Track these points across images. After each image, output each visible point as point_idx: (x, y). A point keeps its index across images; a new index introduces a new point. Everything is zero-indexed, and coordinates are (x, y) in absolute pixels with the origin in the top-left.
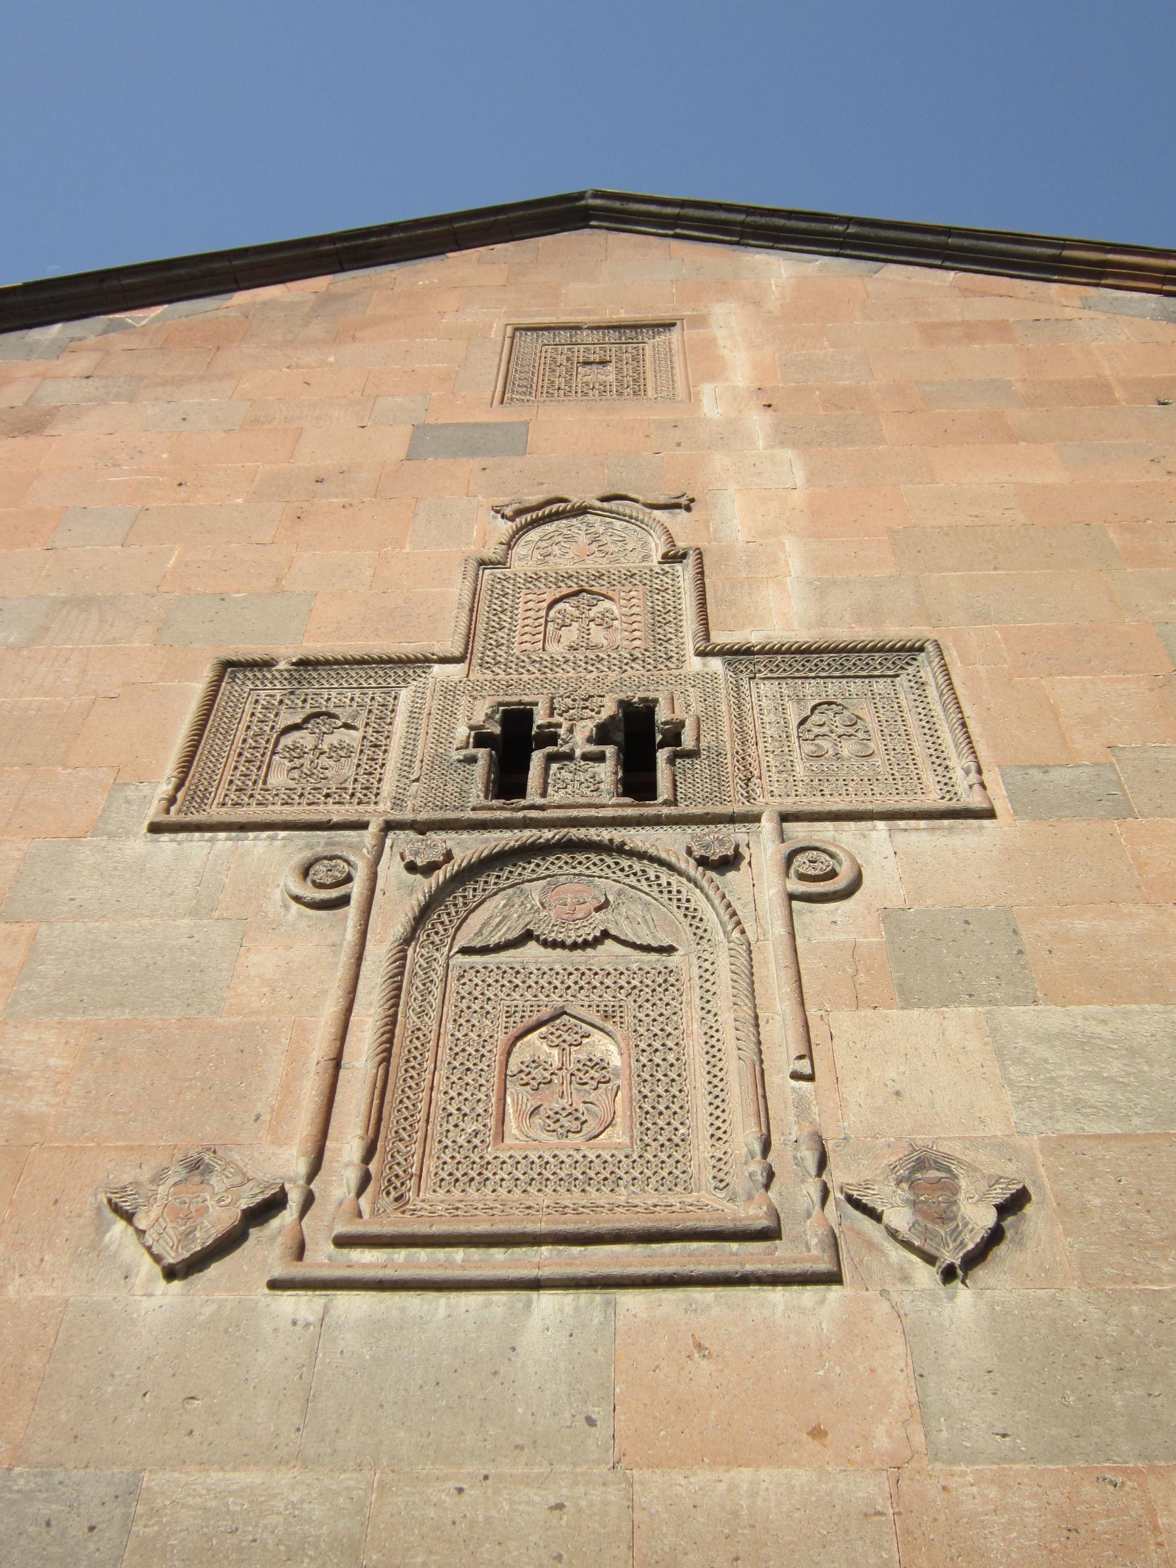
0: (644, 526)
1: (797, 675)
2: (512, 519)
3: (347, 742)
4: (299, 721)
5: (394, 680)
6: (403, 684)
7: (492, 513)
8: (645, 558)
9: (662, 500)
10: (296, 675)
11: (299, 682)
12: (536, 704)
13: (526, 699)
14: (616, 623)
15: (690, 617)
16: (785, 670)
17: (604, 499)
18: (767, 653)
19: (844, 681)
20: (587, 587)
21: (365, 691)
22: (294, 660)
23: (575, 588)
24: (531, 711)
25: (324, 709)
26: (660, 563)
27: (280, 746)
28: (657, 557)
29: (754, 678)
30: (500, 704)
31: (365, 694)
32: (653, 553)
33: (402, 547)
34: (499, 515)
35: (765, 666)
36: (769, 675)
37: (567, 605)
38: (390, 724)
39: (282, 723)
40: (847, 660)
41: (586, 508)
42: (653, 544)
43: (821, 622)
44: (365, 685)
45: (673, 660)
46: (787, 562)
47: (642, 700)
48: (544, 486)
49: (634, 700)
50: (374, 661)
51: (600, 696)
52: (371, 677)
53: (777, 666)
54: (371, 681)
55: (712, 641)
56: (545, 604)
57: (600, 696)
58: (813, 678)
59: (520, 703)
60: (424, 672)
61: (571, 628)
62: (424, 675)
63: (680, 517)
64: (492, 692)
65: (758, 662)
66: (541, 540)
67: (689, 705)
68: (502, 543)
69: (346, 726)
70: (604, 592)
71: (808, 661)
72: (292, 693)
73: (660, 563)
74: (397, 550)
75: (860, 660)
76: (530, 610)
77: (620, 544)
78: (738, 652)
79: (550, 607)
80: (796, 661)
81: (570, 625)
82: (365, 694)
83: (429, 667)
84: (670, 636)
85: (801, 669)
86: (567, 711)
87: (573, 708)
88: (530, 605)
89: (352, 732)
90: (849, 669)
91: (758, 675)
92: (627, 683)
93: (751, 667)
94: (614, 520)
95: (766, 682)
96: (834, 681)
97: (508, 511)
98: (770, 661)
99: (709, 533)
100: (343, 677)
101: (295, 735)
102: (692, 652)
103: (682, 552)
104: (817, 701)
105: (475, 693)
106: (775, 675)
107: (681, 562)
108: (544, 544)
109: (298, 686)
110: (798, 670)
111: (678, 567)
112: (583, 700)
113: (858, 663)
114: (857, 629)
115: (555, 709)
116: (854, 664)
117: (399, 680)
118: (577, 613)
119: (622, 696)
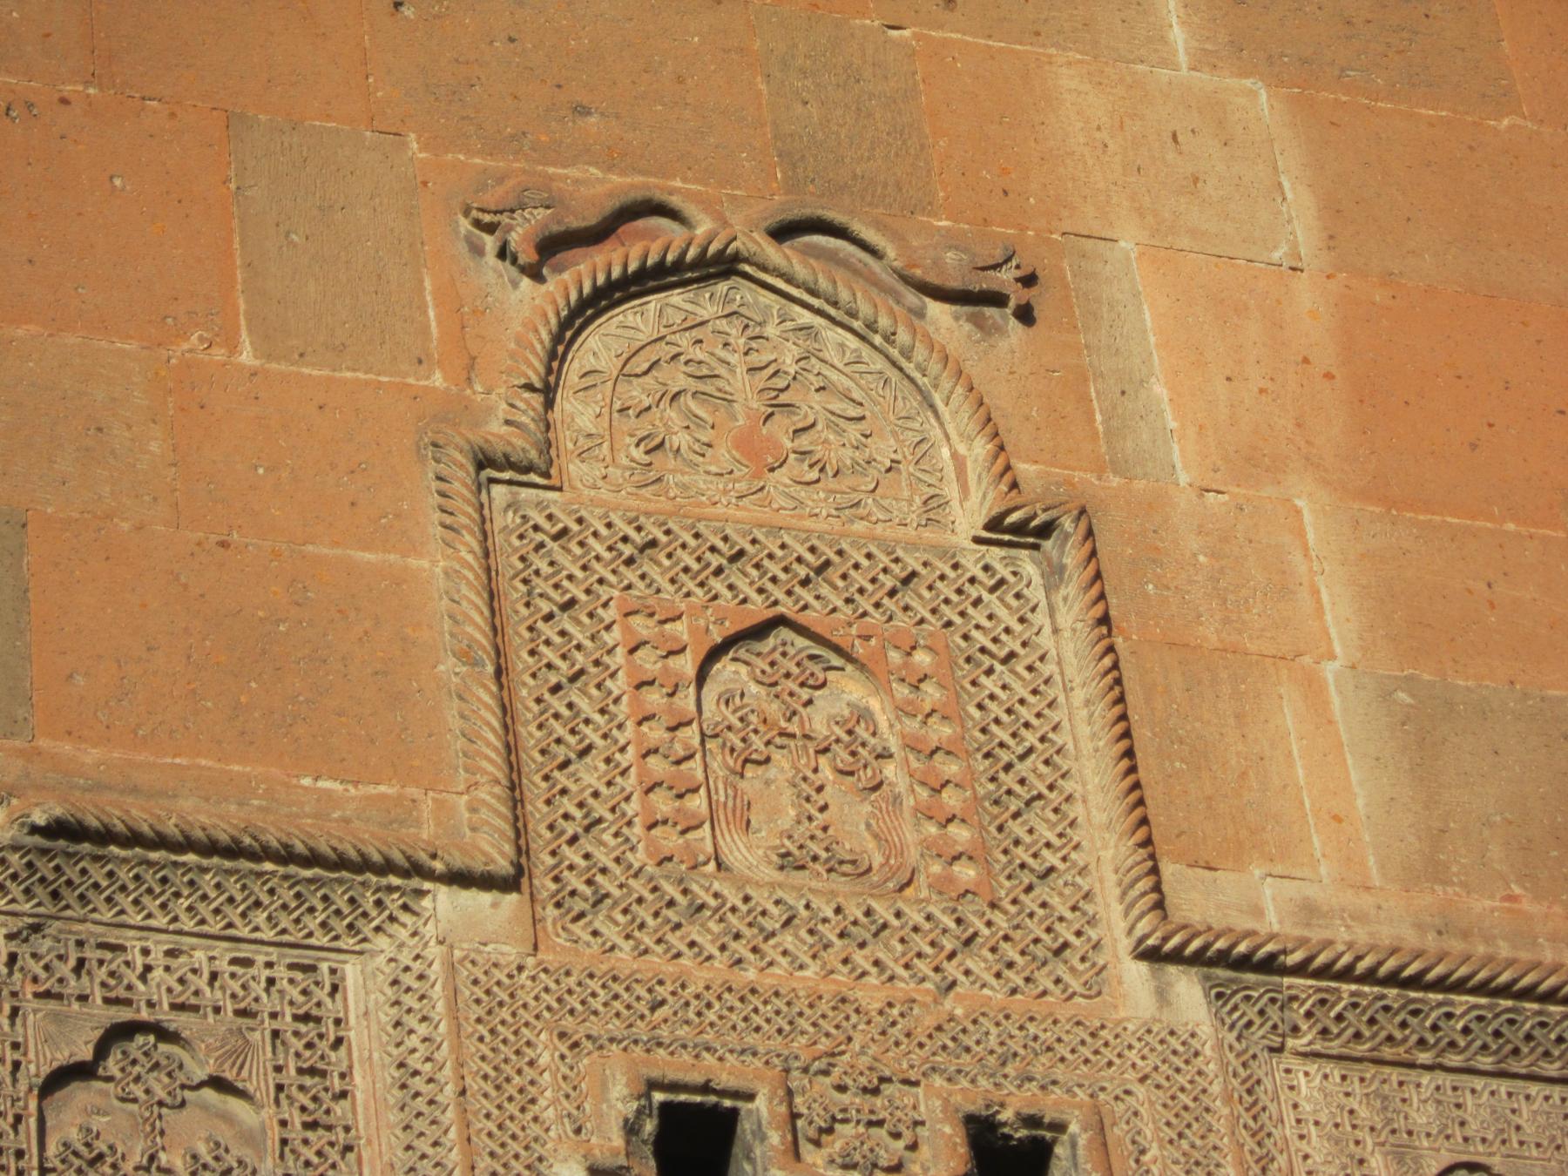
0: (909, 367)
1: (1387, 1052)
2: (535, 274)
3: (236, 1152)
4: (86, 1053)
5: (324, 924)
6: (348, 942)
7: (465, 225)
8: (933, 506)
9: (953, 269)
10: (45, 868)
11: (55, 895)
12: (750, 1097)
13: (724, 1080)
14: (890, 770)
15: (1093, 781)
16: (1358, 1035)
17: (783, 232)
18: (1324, 972)
19: (1503, 1086)
20: (787, 608)
21: (245, 951)
22: (40, 818)
23: (758, 610)
24: (734, 1112)
25: (145, 1015)
26: (978, 540)
27: (52, 1149)
28: (968, 516)
29: (1279, 1050)
30: (653, 1085)
31: (247, 963)
32: (951, 491)
33: (234, 348)
34: (490, 243)
35: (1309, 1014)
36: (1317, 1047)
37: (743, 669)
38: (343, 1095)
39: (38, 1066)
40: (1511, 1022)
41: (737, 258)
42: (945, 452)
43: (1433, 871)
44: (244, 932)
45: (1073, 957)
46: (1316, 592)
47: (1032, 1121)
48: (593, 120)
49: (1002, 1117)
50: (266, 853)
51: (906, 1082)
52: (258, 904)
53: (1339, 1018)
54: (260, 917)
55: (1177, 917)
56: (687, 665)
57: (906, 1082)
58: (1429, 1068)
59: (706, 1088)
60: (405, 907)
61: (771, 772)
62: (405, 918)
63: (1003, 345)
64: (616, 1027)
65: (1293, 998)
66: (624, 375)
67: (1143, 1152)
68: (529, 387)
69: (218, 1083)
70: (844, 644)
71: (1415, 1013)
72: (36, 928)
73: (978, 540)
74: (219, 354)
75: (1543, 1025)
76: (651, 683)
77: (853, 432)
78: (1244, 963)
79: (701, 678)
80: (1386, 1009)
81: (768, 760)
82: (247, 963)
83: (420, 893)
84: (1052, 859)
85: (1398, 1035)
86: (830, 1130)
87: (845, 1121)
88: (648, 661)
89: (234, 1104)
90: (1516, 1051)
91: (1290, 1042)
92: (969, 1041)
93: (1274, 1013)
94: (819, 321)
95: (1312, 1068)
96: (1479, 1083)
97: (522, 233)
98: (1323, 1002)
99: (1095, 435)
100: (177, 895)
101: (80, 1095)
102: (1125, 944)
103: (1042, 518)
104: (1447, 1159)
105: (568, 1023)
106: (1335, 1047)
107: (1036, 547)
108: (637, 393)
109: (53, 911)
110: (1390, 1038)
111: (1028, 565)
112: (865, 1090)
113: (1537, 1033)
114: (1526, 905)
115: (799, 1116)
116: (1529, 1037)
117: (339, 926)
118: (774, 709)
119: (972, 1096)
